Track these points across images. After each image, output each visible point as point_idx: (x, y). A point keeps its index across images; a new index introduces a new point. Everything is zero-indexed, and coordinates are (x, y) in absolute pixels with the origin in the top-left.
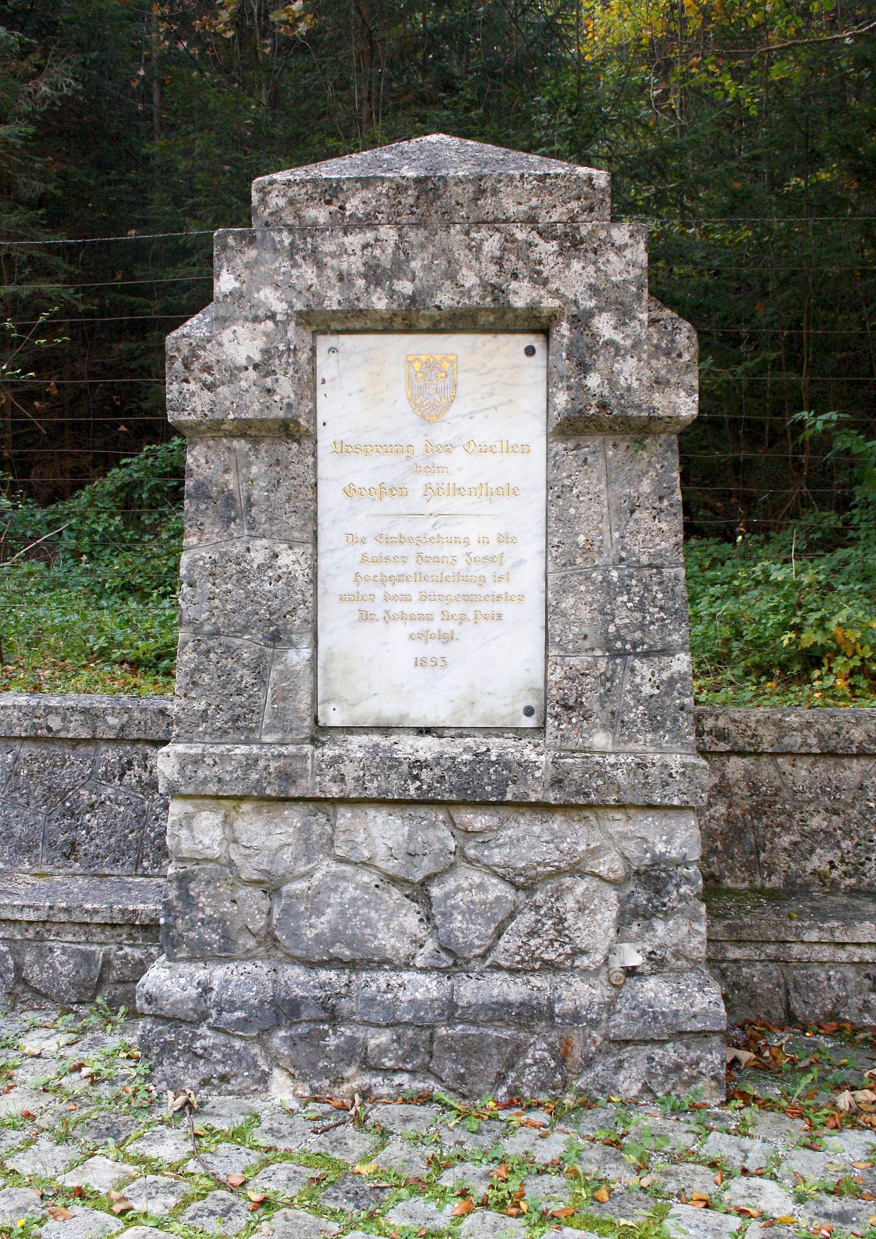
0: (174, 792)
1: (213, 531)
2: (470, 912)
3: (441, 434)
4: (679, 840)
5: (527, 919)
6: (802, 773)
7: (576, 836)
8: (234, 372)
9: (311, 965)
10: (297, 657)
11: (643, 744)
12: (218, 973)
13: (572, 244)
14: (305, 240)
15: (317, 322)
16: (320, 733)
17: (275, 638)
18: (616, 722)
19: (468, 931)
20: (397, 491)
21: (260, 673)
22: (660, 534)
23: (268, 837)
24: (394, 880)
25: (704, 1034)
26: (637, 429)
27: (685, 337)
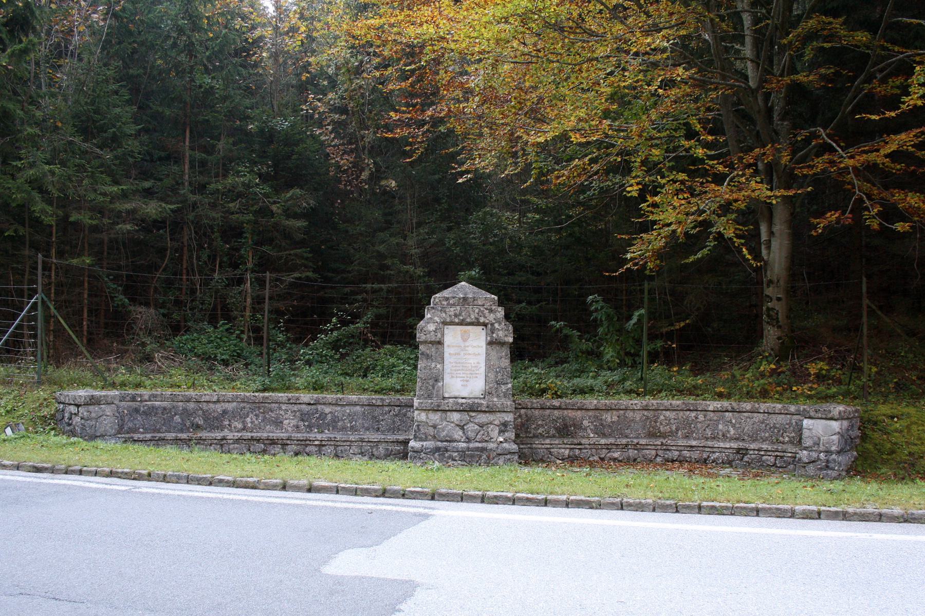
0: (417, 409)
1: (425, 361)
2: (472, 431)
3: (467, 344)
4: (509, 417)
5: (482, 432)
6: (537, 412)
7: (491, 417)
8: (430, 332)
9: (442, 441)
10: (440, 384)
11: (503, 400)
12: (425, 443)
13: (491, 311)
14: (443, 310)
15: (445, 323)
16: (444, 398)
17: (436, 381)
18: (498, 396)
19: (471, 435)
20: (459, 354)
21: (433, 388)
22: (506, 362)
23: (435, 417)
24: (457, 425)
25: (514, 453)
26: (502, 344)
27: (511, 328)
